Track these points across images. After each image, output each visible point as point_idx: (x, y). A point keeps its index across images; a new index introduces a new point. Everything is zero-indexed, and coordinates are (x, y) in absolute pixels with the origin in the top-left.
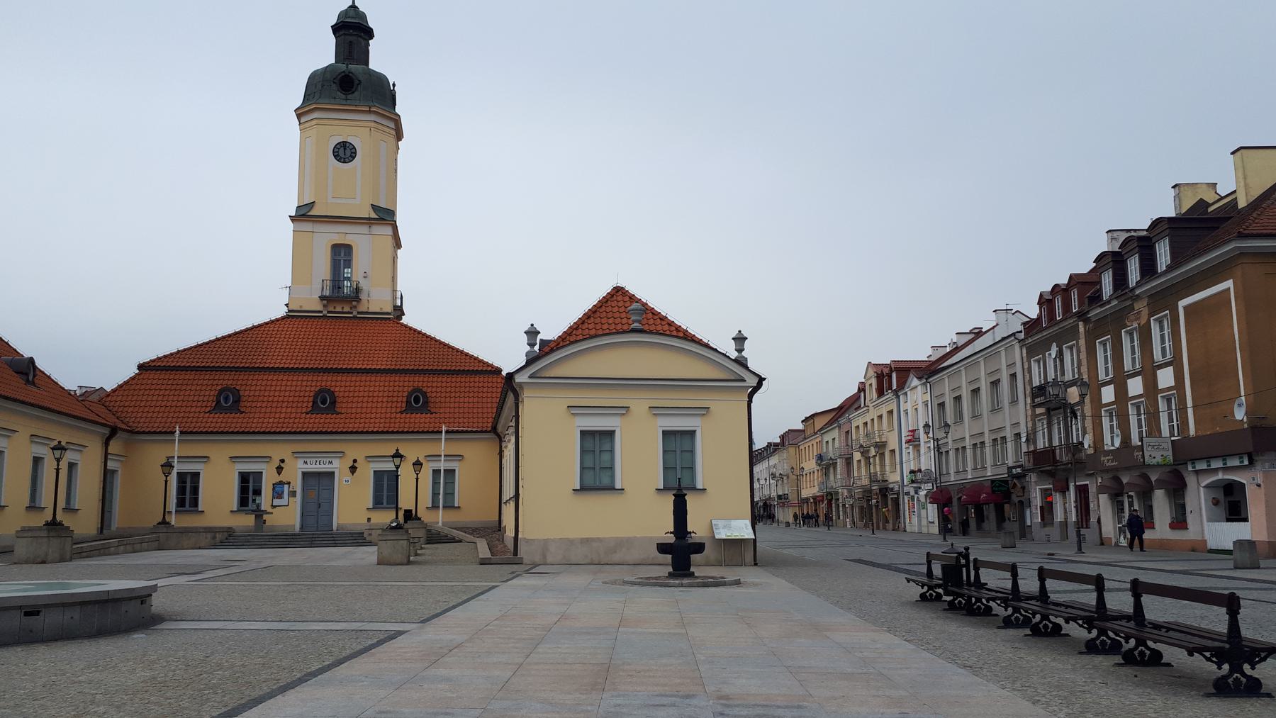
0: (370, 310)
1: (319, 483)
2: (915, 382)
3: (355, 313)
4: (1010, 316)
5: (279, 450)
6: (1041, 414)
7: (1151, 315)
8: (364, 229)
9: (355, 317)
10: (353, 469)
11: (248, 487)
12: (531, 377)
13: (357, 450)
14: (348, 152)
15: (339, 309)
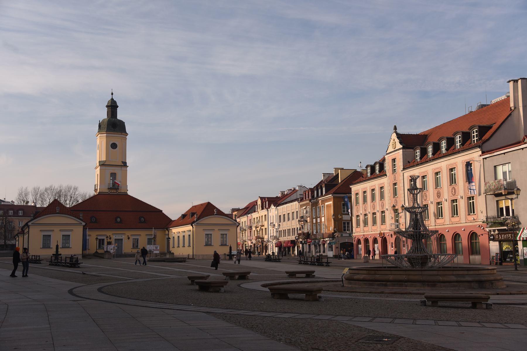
0: (122, 192)
1: (119, 241)
2: (273, 206)
3: (117, 193)
4: (302, 188)
5: (109, 233)
6: (302, 223)
7: (321, 205)
8: (119, 168)
9: (118, 194)
10: (129, 238)
11: (101, 242)
12: (197, 224)
13: (129, 233)
14: (115, 146)
15: (113, 192)
